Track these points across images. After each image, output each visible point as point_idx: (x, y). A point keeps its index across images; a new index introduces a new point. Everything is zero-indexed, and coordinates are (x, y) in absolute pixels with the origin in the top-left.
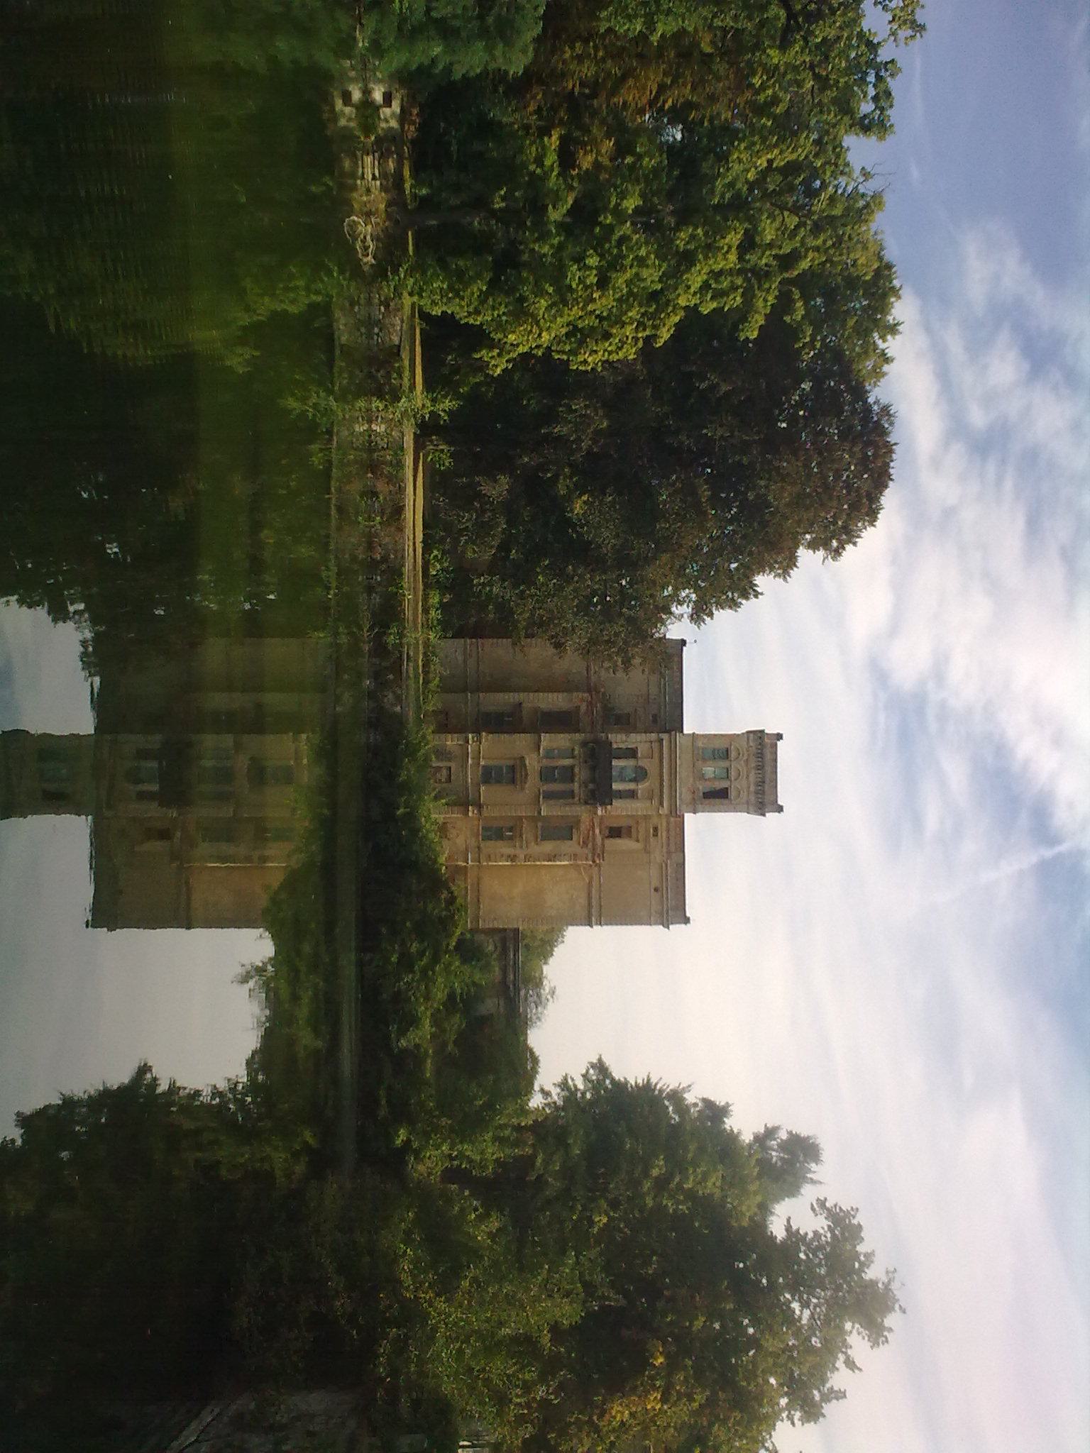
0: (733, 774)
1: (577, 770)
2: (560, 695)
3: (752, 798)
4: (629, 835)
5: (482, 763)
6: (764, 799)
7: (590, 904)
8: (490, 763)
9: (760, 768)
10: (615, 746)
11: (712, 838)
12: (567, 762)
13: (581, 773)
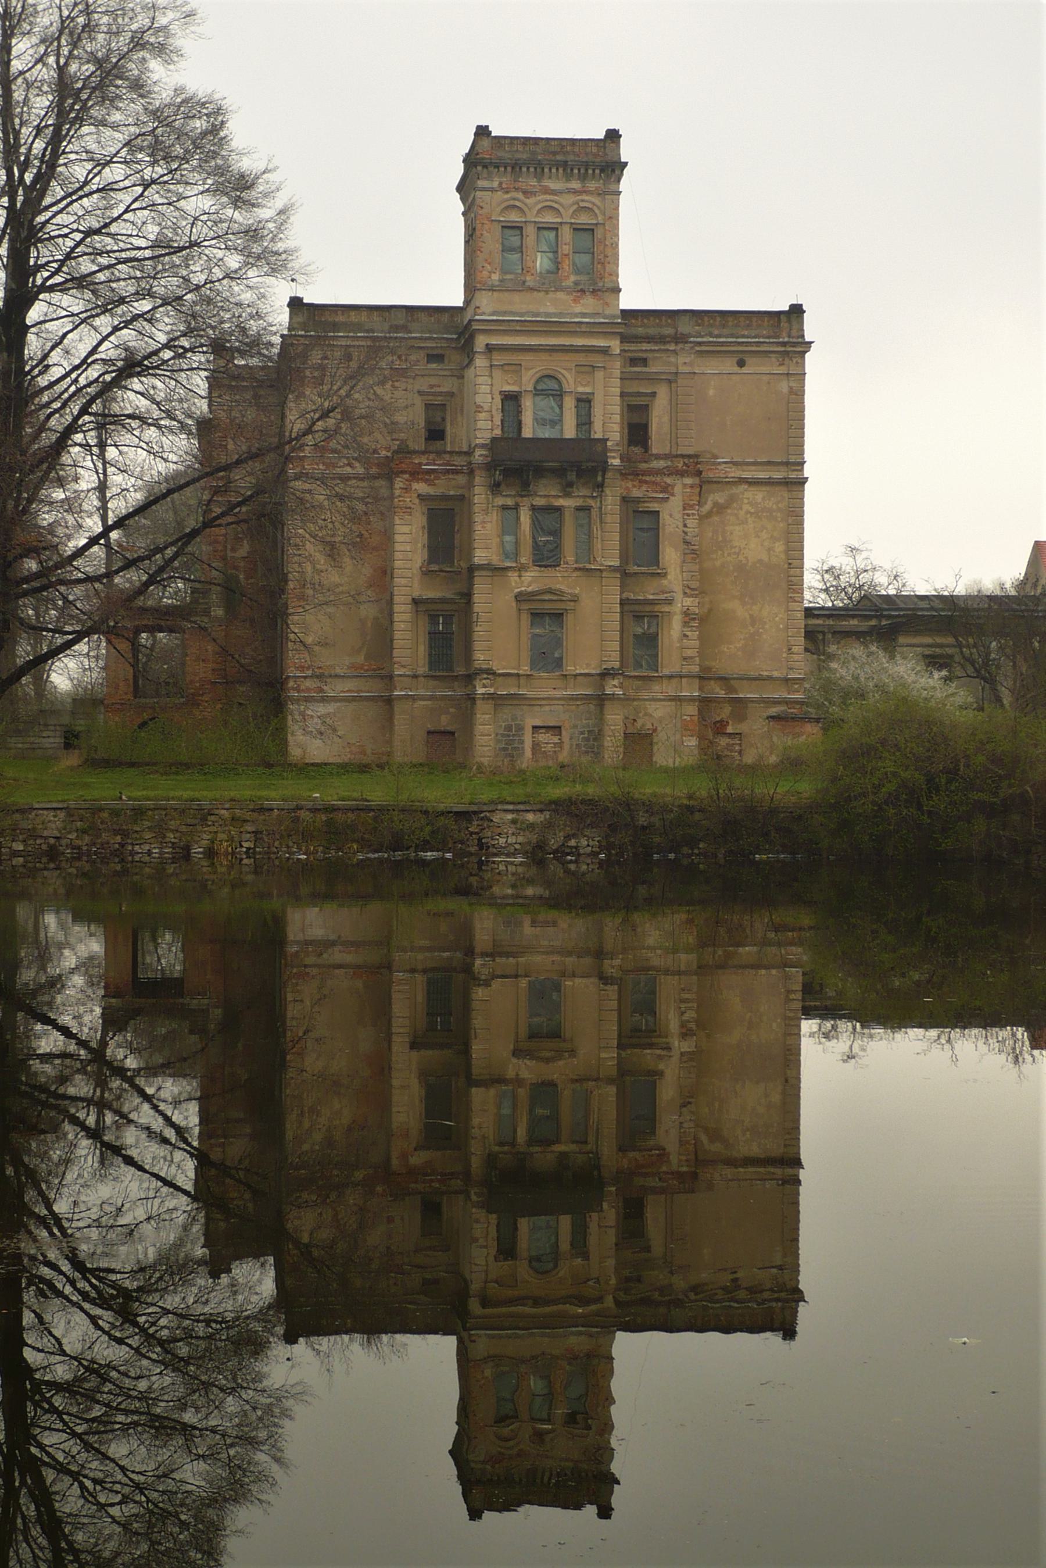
0: (549, 218)
1: (539, 502)
2: (399, 529)
3: (592, 185)
4: (645, 409)
5: (525, 669)
6: (597, 162)
7: (769, 482)
8: (526, 655)
9: (539, 169)
10: (498, 432)
11: (665, 260)
12: (525, 518)
13: (547, 492)
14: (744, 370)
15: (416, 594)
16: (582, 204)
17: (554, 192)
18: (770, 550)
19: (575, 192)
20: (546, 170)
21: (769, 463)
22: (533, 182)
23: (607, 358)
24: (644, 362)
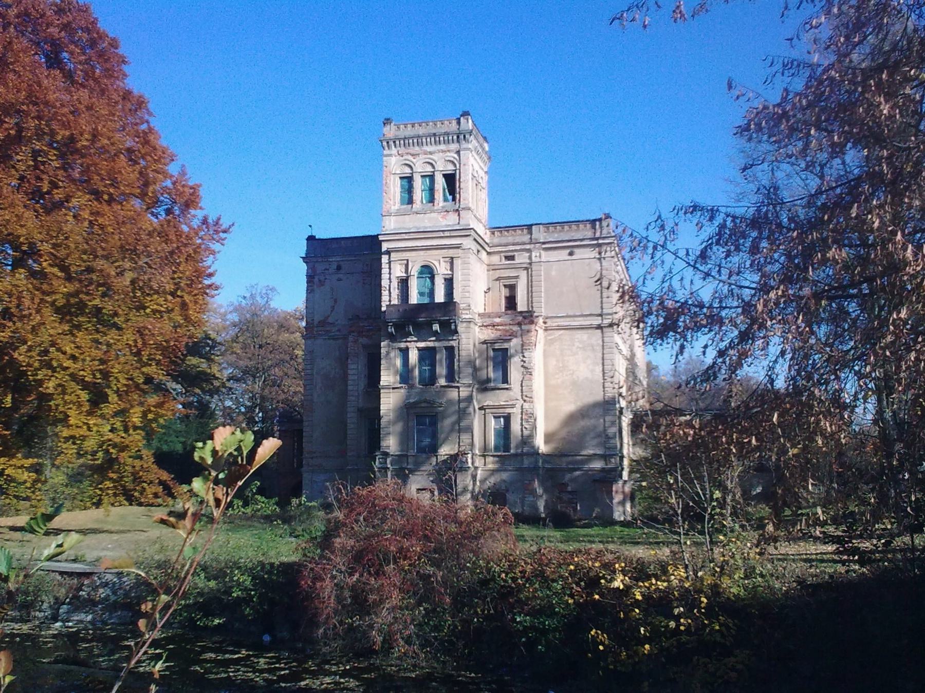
14: (573, 257)
15: (361, 405)
16: (447, 159)
17: (431, 153)
18: (592, 371)
19: (443, 151)
20: (424, 140)
21: (590, 315)
22: (417, 148)
23: (460, 251)
24: (512, 258)
